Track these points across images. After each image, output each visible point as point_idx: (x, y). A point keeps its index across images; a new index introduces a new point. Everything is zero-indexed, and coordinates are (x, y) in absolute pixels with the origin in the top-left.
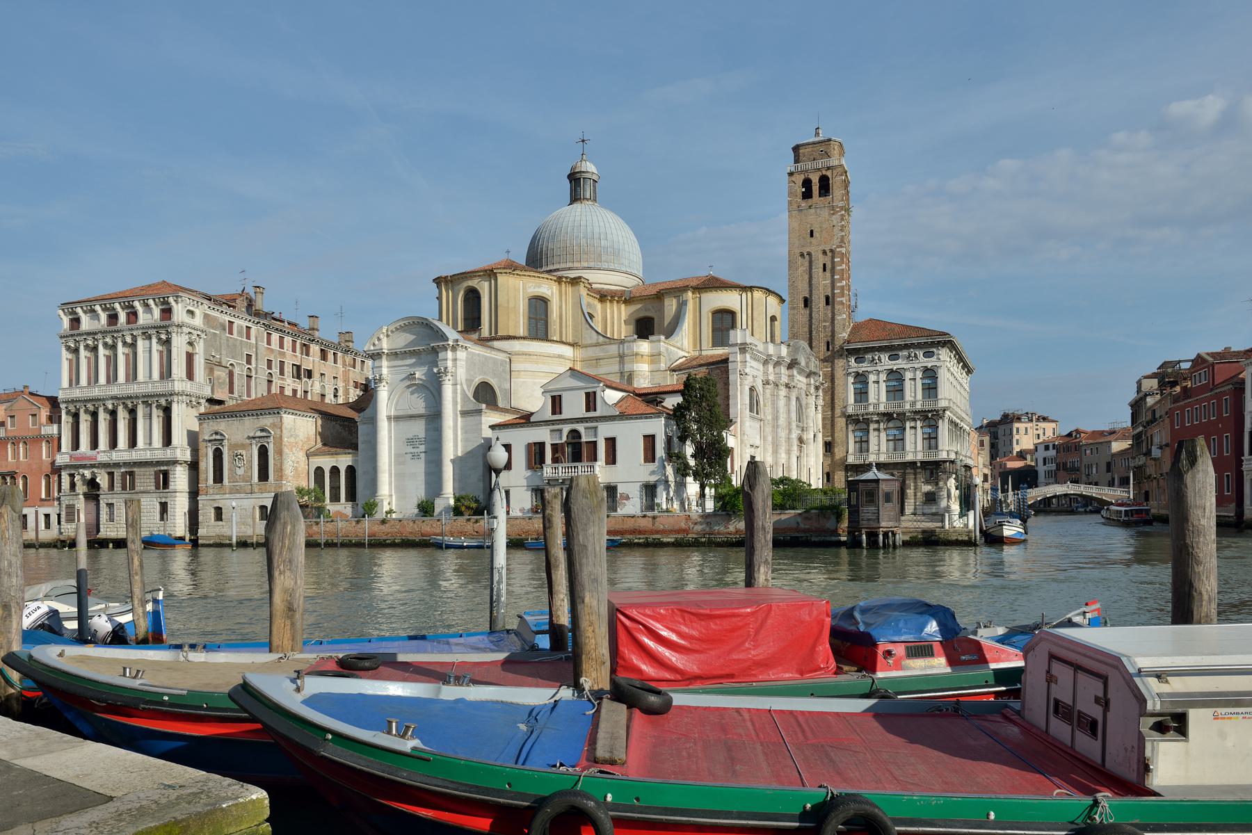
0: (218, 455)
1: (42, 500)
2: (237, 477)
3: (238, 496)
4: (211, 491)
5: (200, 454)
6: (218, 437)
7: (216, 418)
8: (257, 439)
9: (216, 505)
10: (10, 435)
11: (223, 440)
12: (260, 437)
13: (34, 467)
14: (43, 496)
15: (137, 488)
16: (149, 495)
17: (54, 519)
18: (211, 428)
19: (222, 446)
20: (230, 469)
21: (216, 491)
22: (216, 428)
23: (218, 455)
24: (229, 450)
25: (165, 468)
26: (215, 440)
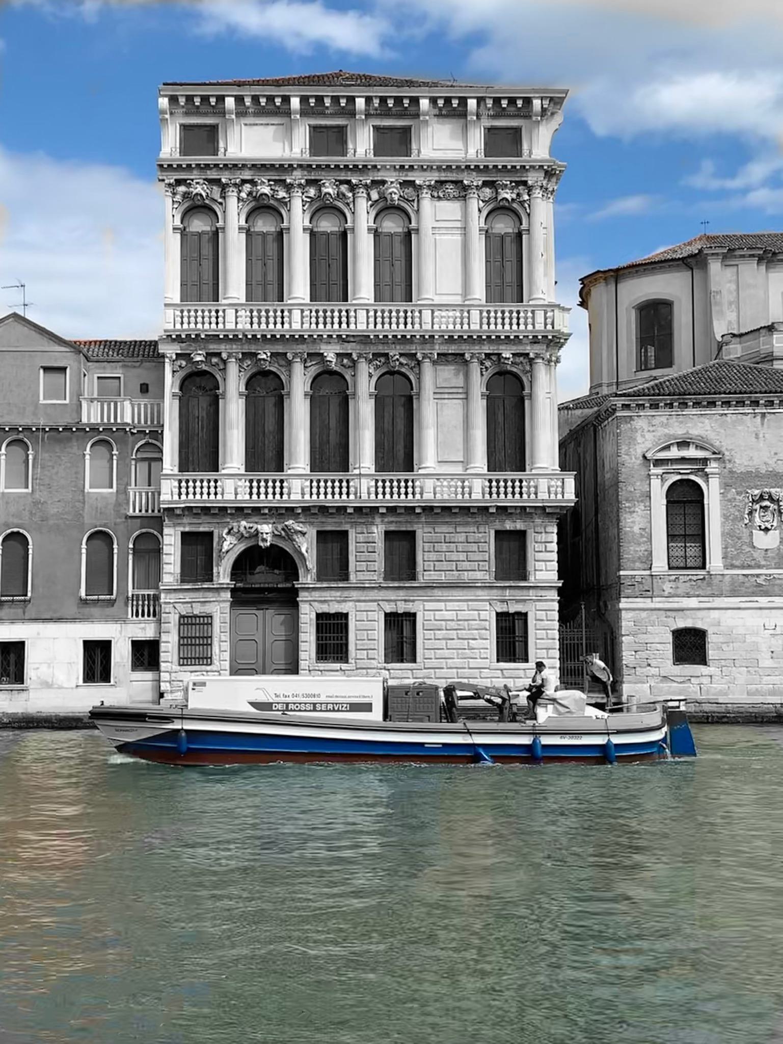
1: (84, 602)
3: (763, 601)
4: (667, 587)
5: (623, 494)
6: (692, 452)
7: (684, 405)
9: (681, 624)
11: (705, 461)
13: (53, 510)
14: (83, 593)
17: (121, 655)
18: (662, 431)
19: (706, 476)
20: (728, 535)
24: (726, 486)
25: (519, 525)
26: (683, 460)
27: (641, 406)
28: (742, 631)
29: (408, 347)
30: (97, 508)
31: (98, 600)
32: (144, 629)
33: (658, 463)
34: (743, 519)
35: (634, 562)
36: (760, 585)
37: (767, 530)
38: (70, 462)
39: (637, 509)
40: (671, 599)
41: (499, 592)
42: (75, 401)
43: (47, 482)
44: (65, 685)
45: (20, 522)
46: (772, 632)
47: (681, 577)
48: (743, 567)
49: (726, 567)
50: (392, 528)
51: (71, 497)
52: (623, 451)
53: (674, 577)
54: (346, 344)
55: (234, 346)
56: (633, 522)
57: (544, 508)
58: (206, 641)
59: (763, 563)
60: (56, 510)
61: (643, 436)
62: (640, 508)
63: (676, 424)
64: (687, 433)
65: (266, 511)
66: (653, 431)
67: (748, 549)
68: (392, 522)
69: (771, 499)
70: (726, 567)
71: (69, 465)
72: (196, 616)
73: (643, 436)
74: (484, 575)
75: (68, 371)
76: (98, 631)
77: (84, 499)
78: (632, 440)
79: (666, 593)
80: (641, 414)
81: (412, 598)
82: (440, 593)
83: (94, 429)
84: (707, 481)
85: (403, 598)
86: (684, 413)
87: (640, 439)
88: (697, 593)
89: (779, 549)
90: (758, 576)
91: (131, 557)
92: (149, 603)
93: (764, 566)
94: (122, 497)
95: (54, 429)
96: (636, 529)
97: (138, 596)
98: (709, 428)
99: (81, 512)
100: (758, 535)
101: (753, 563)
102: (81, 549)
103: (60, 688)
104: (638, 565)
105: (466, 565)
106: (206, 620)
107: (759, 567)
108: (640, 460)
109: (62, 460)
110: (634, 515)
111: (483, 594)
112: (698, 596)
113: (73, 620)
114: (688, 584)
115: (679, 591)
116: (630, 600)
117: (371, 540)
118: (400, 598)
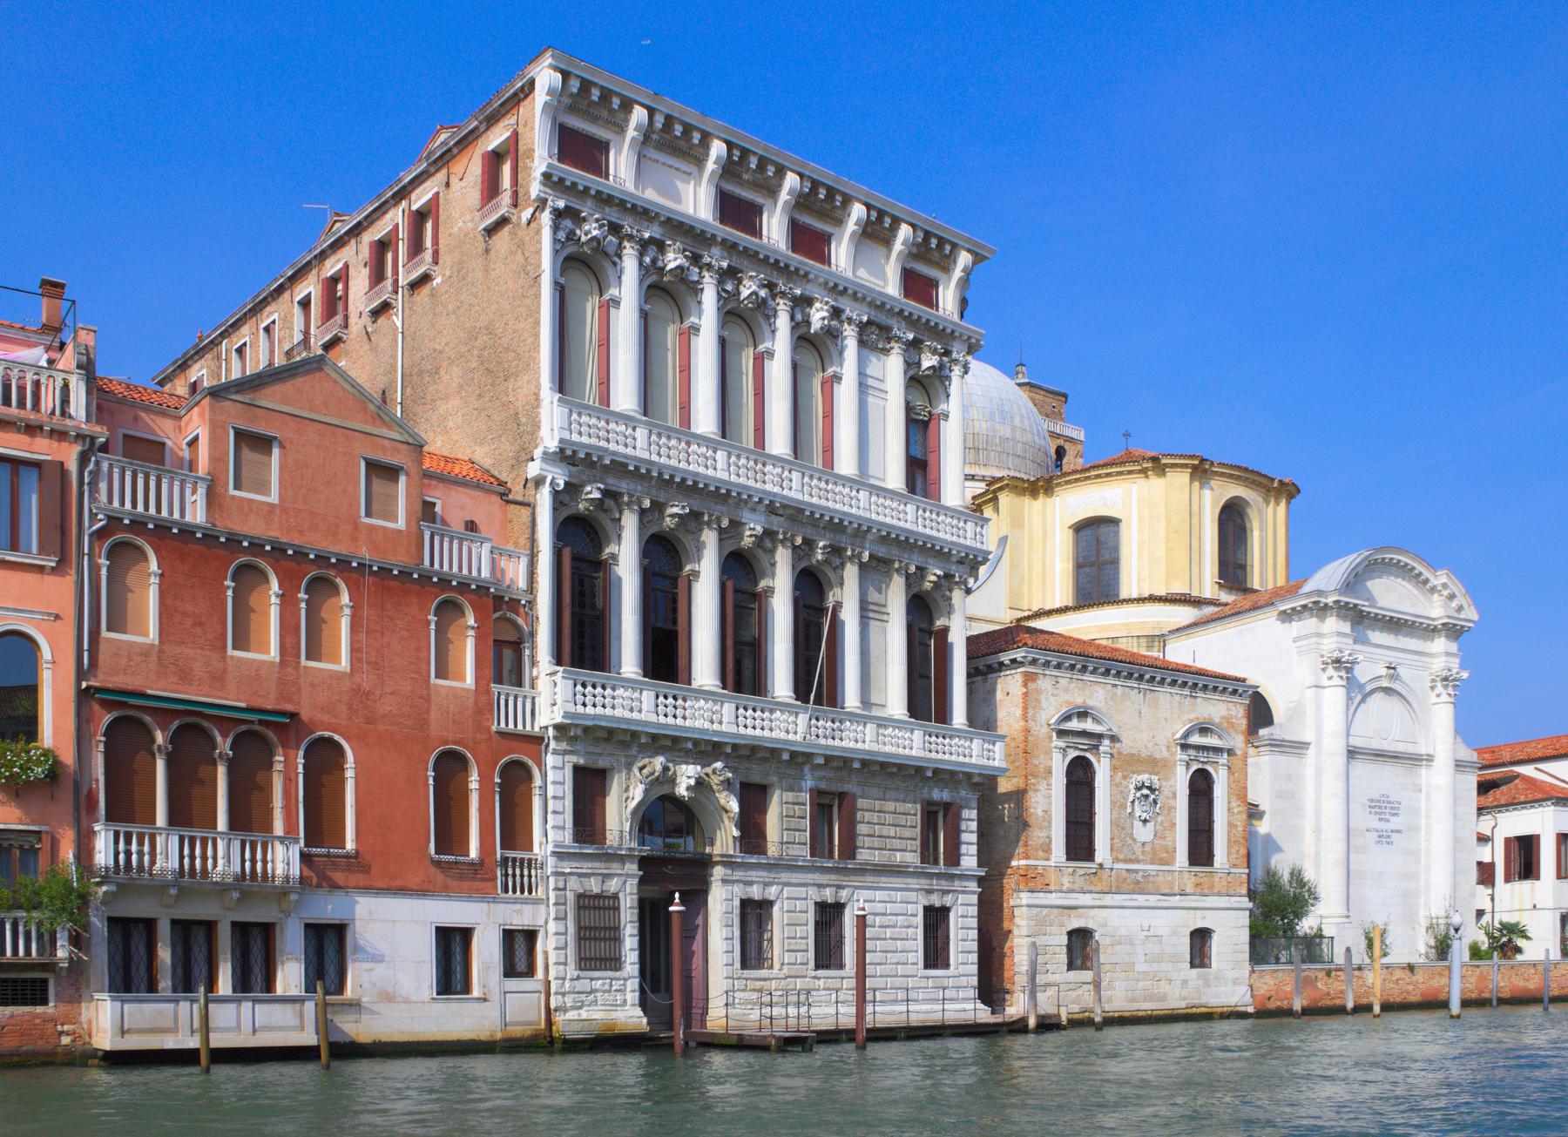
0: (1080, 779)
2: (1137, 848)
3: (1141, 899)
4: (1066, 881)
6: (1089, 725)
7: (1084, 669)
8: (1192, 752)
9: (1076, 923)
10: (252, 527)
12: (1199, 748)
15: (863, 855)
16: (897, 882)
17: (486, 953)
19: (1097, 754)
21: (1080, 882)
22: (1079, 700)
23: (1080, 779)
24: (1114, 768)
27: (1047, 664)
28: (1123, 932)
29: (838, 538)
30: (448, 712)
31: (456, 862)
32: (519, 912)
33: (1062, 733)
34: (1126, 808)
35: (1037, 850)
36: (1138, 882)
37: (1145, 821)
38: (407, 631)
39: (1040, 787)
40: (1069, 895)
41: (928, 881)
42: (414, 530)
43: (374, 659)
44: (414, 998)
45: (333, 721)
46: (1146, 933)
47: (1078, 870)
48: (1126, 861)
49: (1116, 860)
50: (823, 786)
51: (409, 688)
52: (1030, 715)
53: (1071, 870)
54: (773, 516)
55: (639, 488)
56: (1037, 802)
57: (969, 776)
58: (613, 935)
59: (1141, 857)
60: (388, 708)
61: (1047, 699)
62: (1042, 786)
63: (1076, 690)
64: (1084, 702)
65: (690, 746)
66: (1056, 695)
67: (1130, 842)
68: (821, 779)
69: (1149, 788)
70: (1116, 860)
71: (406, 634)
72: (598, 896)
73: (1047, 699)
74: (912, 858)
75: (402, 479)
76: (455, 912)
77: (428, 695)
78: (1038, 701)
79: (1064, 888)
80: (1047, 672)
81: (844, 883)
82: (871, 879)
83: (444, 582)
84: (1099, 761)
85: (836, 883)
86: (1084, 678)
87: (1044, 703)
88: (1090, 888)
89: (1152, 842)
90: (1136, 871)
91: (497, 797)
92: (530, 872)
93: (1143, 861)
94: (484, 698)
95: (385, 571)
96: (1040, 812)
97: (507, 858)
98: (1103, 701)
99: (425, 716)
100: (1138, 824)
101: (1133, 857)
102: (427, 778)
103: (407, 1001)
104: (1041, 853)
105: (897, 843)
106: (608, 903)
107: (1138, 861)
108: (1045, 730)
109: (395, 625)
110: (1039, 794)
111: (913, 883)
112: (1091, 892)
113: (422, 892)
114: (1082, 878)
115: (1076, 887)
116: (1035, 895)
117: (800, 800)
118: (832, 883)
